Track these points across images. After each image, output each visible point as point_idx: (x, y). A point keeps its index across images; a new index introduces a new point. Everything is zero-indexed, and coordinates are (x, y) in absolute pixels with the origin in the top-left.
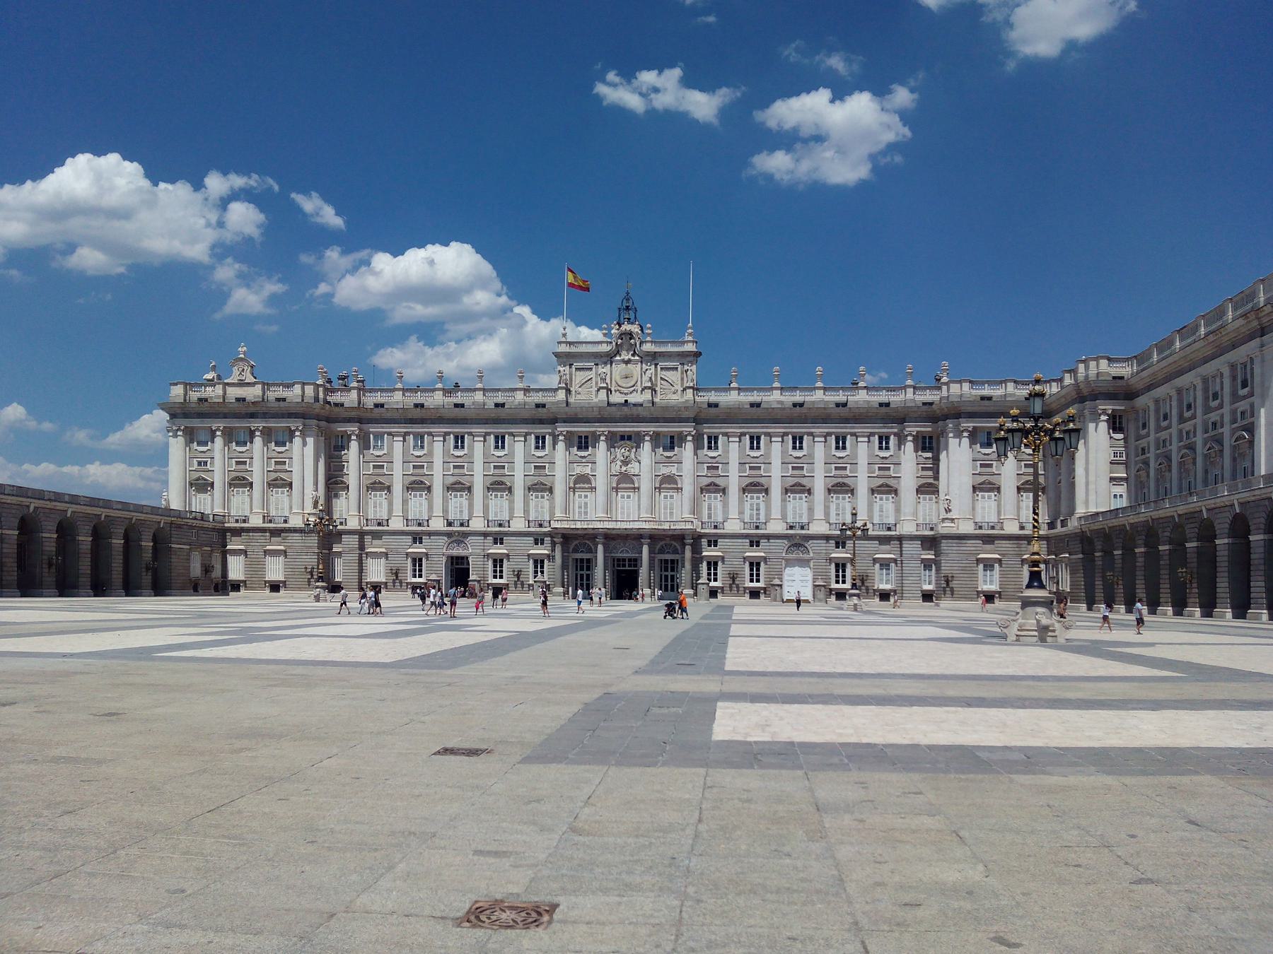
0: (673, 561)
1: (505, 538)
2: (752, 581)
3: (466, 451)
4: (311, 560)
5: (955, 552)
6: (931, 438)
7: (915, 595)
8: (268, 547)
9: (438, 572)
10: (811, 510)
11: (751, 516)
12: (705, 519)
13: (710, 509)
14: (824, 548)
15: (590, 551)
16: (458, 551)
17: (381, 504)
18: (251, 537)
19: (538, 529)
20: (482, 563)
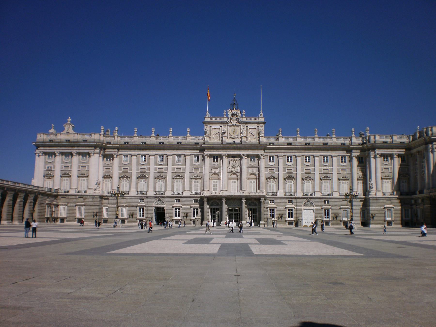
0: (254, 209)
1: (180, 200)
2: (289, 217)
3: (164, 162)
4: (96, 209)
5: (375, 204)
6: (362, 158)
7: (358, 223)
8: (78, 203)
9: (151, 214)
10: (314, 188)
11: (288, 190)
12: (269, 191)
13: (270, 187)
14: (320, 203)
15: (218, 205)
16: (160, 206)
17: (126, 184)
18: (70, 199)
19: (196, 196)
20: (170, 210)
